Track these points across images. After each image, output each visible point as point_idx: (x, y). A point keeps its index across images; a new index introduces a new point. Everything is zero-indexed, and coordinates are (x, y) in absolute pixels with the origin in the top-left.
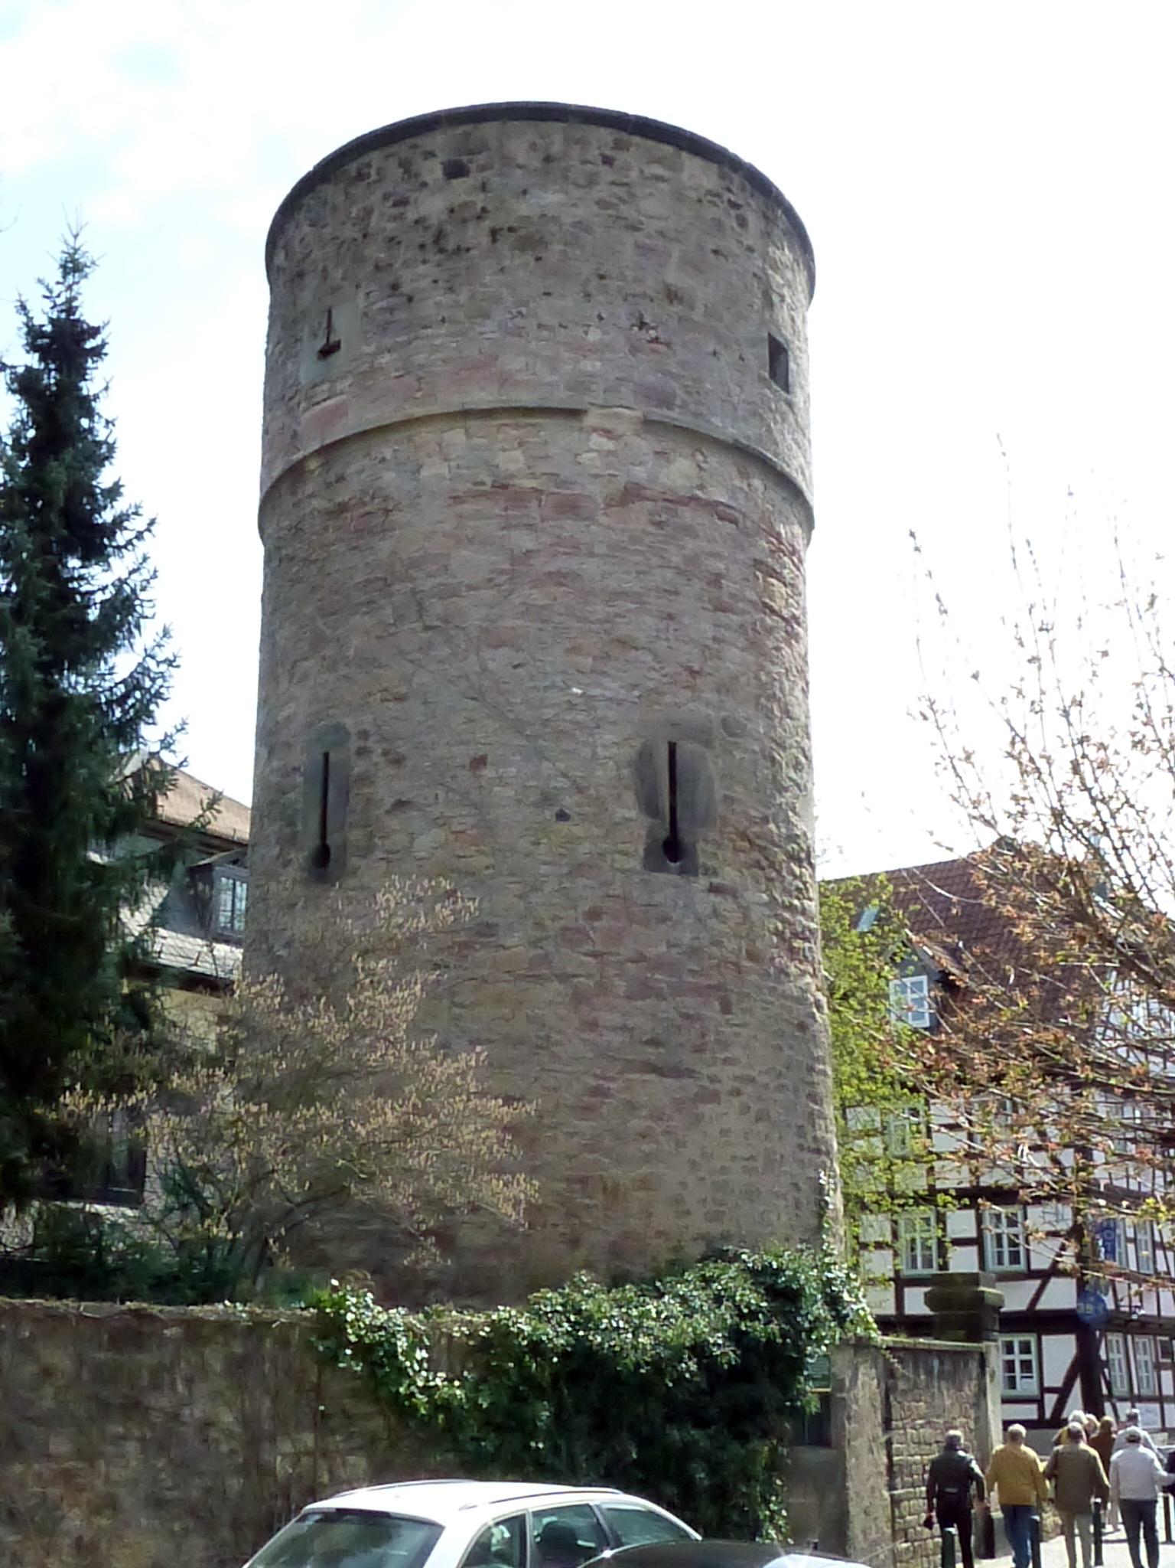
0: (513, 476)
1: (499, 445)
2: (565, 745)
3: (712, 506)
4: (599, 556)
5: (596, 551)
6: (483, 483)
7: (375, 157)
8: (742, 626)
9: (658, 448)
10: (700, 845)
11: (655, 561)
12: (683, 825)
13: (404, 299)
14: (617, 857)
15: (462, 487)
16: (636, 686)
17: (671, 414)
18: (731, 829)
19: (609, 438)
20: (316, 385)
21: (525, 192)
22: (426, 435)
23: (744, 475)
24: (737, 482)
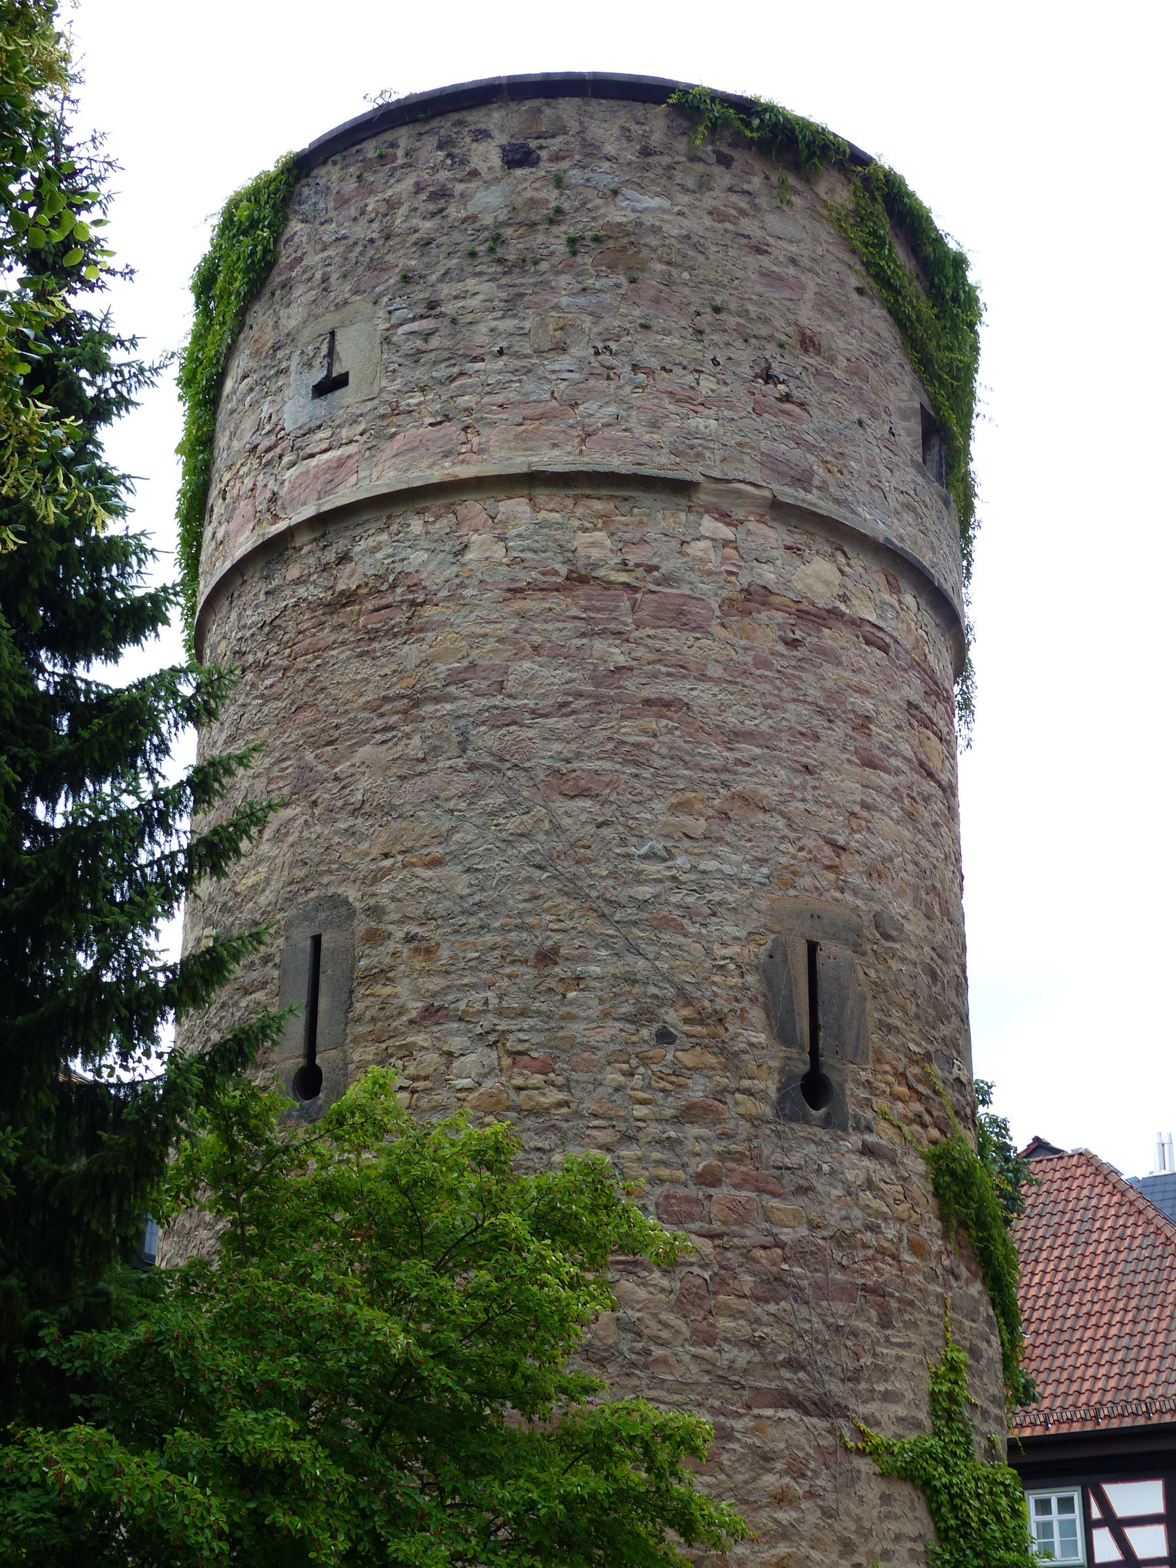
0: (595, 566)
1: (576, 523)
2: (666, 937)
3: (856, 623)
4: (710, 679)
5: (709, 673)
6: (556, 573)
7: (403, 136)
8: (895, 789)
9: (789, 541)
10: (850, 1086)
11: (787, 693)
12: (827, 1059)
13: (447, 321)
14: (738, 1095)
15: (524, 577)
16: (762, 861)
17: (809, 497)
18: (887, 1068)
19: (728, 524)
20: (311, 431)
21: (615, 193)
22: (474, 508)
23: (894, 589)
24: (886, 597)
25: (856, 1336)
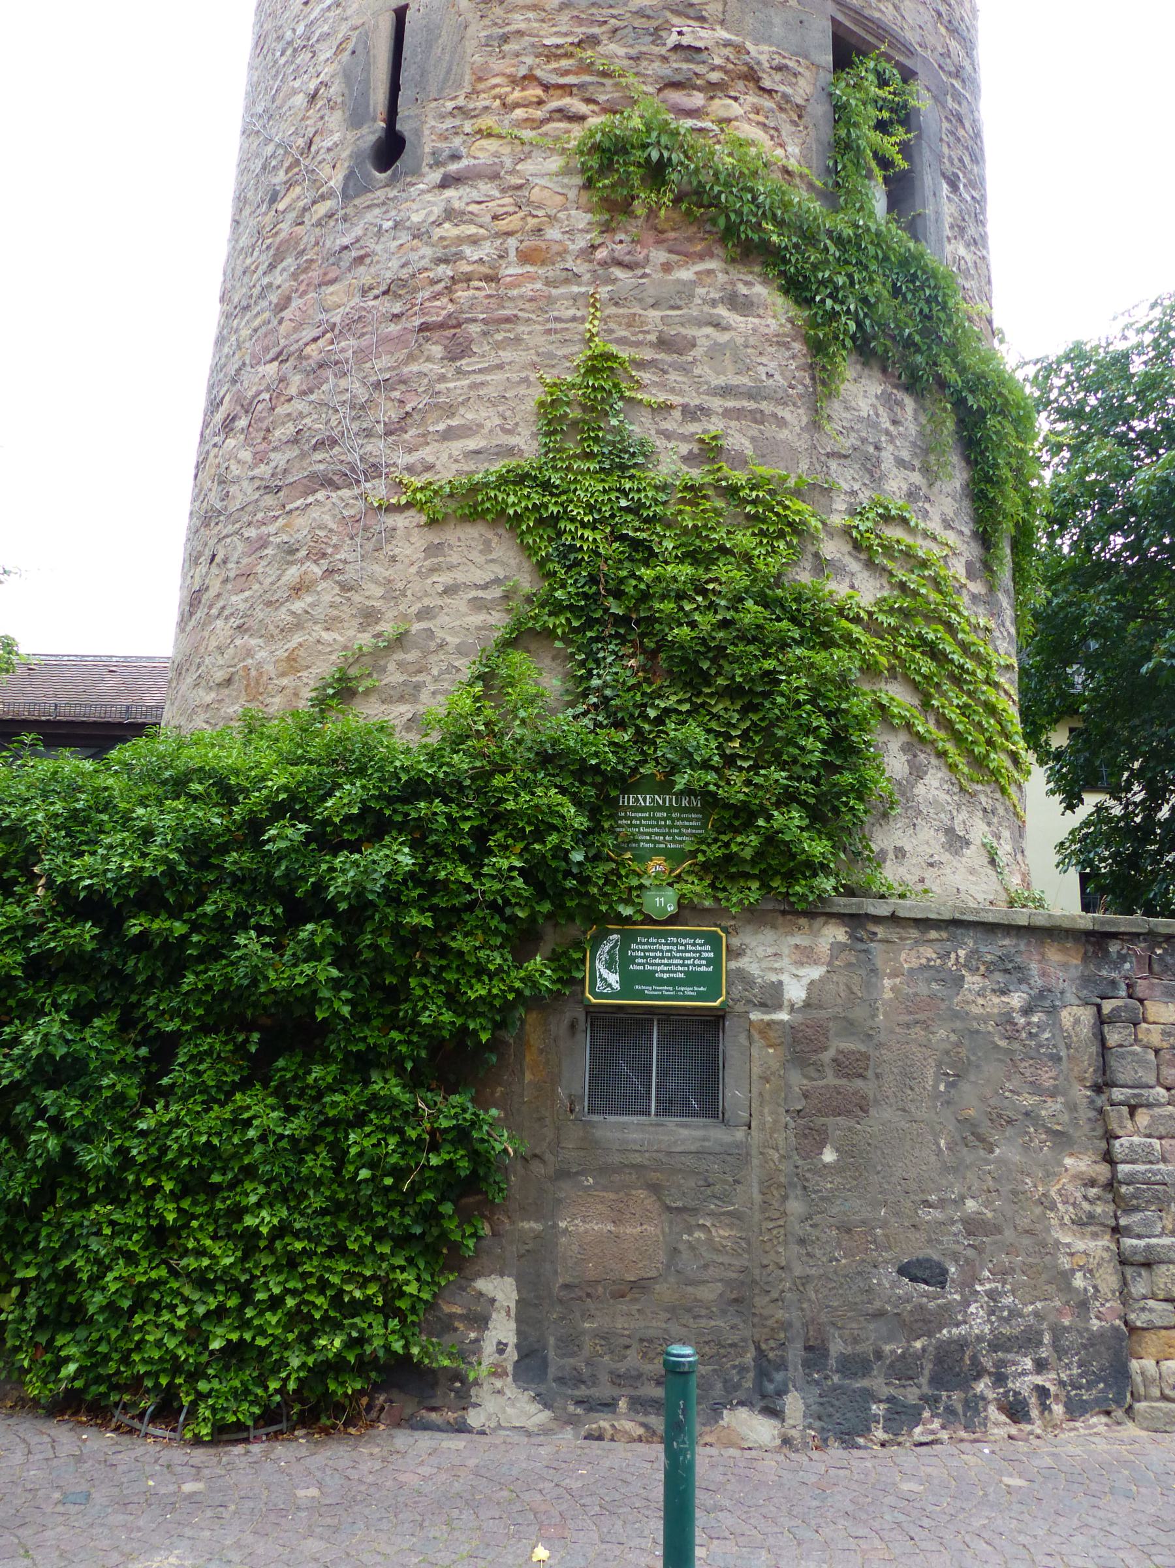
25: (404, 382)
